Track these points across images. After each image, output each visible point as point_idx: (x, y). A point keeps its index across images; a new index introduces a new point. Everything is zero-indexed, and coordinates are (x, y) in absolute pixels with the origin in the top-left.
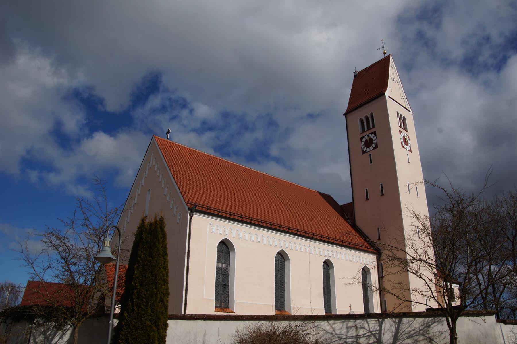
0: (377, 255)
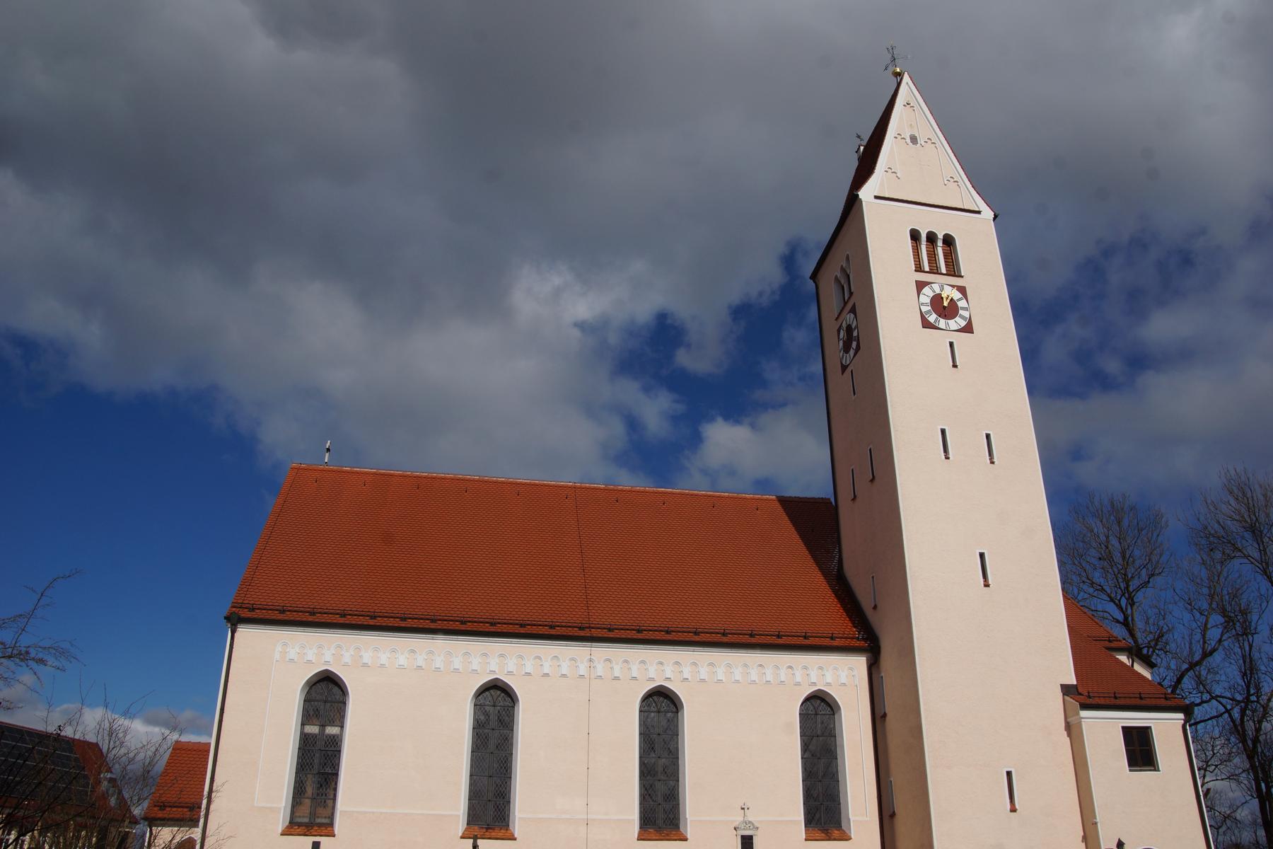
0: (869, 654)
